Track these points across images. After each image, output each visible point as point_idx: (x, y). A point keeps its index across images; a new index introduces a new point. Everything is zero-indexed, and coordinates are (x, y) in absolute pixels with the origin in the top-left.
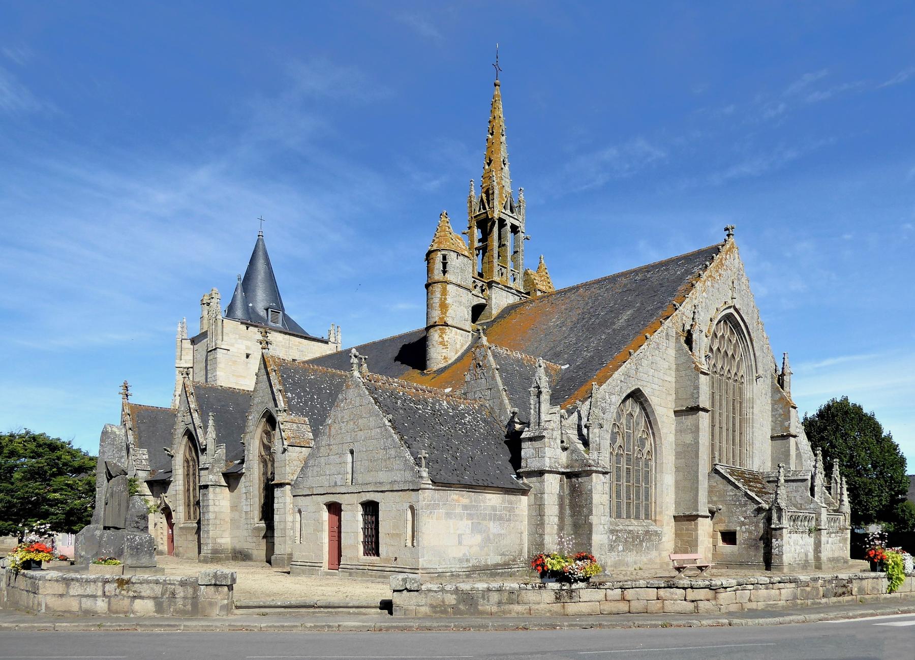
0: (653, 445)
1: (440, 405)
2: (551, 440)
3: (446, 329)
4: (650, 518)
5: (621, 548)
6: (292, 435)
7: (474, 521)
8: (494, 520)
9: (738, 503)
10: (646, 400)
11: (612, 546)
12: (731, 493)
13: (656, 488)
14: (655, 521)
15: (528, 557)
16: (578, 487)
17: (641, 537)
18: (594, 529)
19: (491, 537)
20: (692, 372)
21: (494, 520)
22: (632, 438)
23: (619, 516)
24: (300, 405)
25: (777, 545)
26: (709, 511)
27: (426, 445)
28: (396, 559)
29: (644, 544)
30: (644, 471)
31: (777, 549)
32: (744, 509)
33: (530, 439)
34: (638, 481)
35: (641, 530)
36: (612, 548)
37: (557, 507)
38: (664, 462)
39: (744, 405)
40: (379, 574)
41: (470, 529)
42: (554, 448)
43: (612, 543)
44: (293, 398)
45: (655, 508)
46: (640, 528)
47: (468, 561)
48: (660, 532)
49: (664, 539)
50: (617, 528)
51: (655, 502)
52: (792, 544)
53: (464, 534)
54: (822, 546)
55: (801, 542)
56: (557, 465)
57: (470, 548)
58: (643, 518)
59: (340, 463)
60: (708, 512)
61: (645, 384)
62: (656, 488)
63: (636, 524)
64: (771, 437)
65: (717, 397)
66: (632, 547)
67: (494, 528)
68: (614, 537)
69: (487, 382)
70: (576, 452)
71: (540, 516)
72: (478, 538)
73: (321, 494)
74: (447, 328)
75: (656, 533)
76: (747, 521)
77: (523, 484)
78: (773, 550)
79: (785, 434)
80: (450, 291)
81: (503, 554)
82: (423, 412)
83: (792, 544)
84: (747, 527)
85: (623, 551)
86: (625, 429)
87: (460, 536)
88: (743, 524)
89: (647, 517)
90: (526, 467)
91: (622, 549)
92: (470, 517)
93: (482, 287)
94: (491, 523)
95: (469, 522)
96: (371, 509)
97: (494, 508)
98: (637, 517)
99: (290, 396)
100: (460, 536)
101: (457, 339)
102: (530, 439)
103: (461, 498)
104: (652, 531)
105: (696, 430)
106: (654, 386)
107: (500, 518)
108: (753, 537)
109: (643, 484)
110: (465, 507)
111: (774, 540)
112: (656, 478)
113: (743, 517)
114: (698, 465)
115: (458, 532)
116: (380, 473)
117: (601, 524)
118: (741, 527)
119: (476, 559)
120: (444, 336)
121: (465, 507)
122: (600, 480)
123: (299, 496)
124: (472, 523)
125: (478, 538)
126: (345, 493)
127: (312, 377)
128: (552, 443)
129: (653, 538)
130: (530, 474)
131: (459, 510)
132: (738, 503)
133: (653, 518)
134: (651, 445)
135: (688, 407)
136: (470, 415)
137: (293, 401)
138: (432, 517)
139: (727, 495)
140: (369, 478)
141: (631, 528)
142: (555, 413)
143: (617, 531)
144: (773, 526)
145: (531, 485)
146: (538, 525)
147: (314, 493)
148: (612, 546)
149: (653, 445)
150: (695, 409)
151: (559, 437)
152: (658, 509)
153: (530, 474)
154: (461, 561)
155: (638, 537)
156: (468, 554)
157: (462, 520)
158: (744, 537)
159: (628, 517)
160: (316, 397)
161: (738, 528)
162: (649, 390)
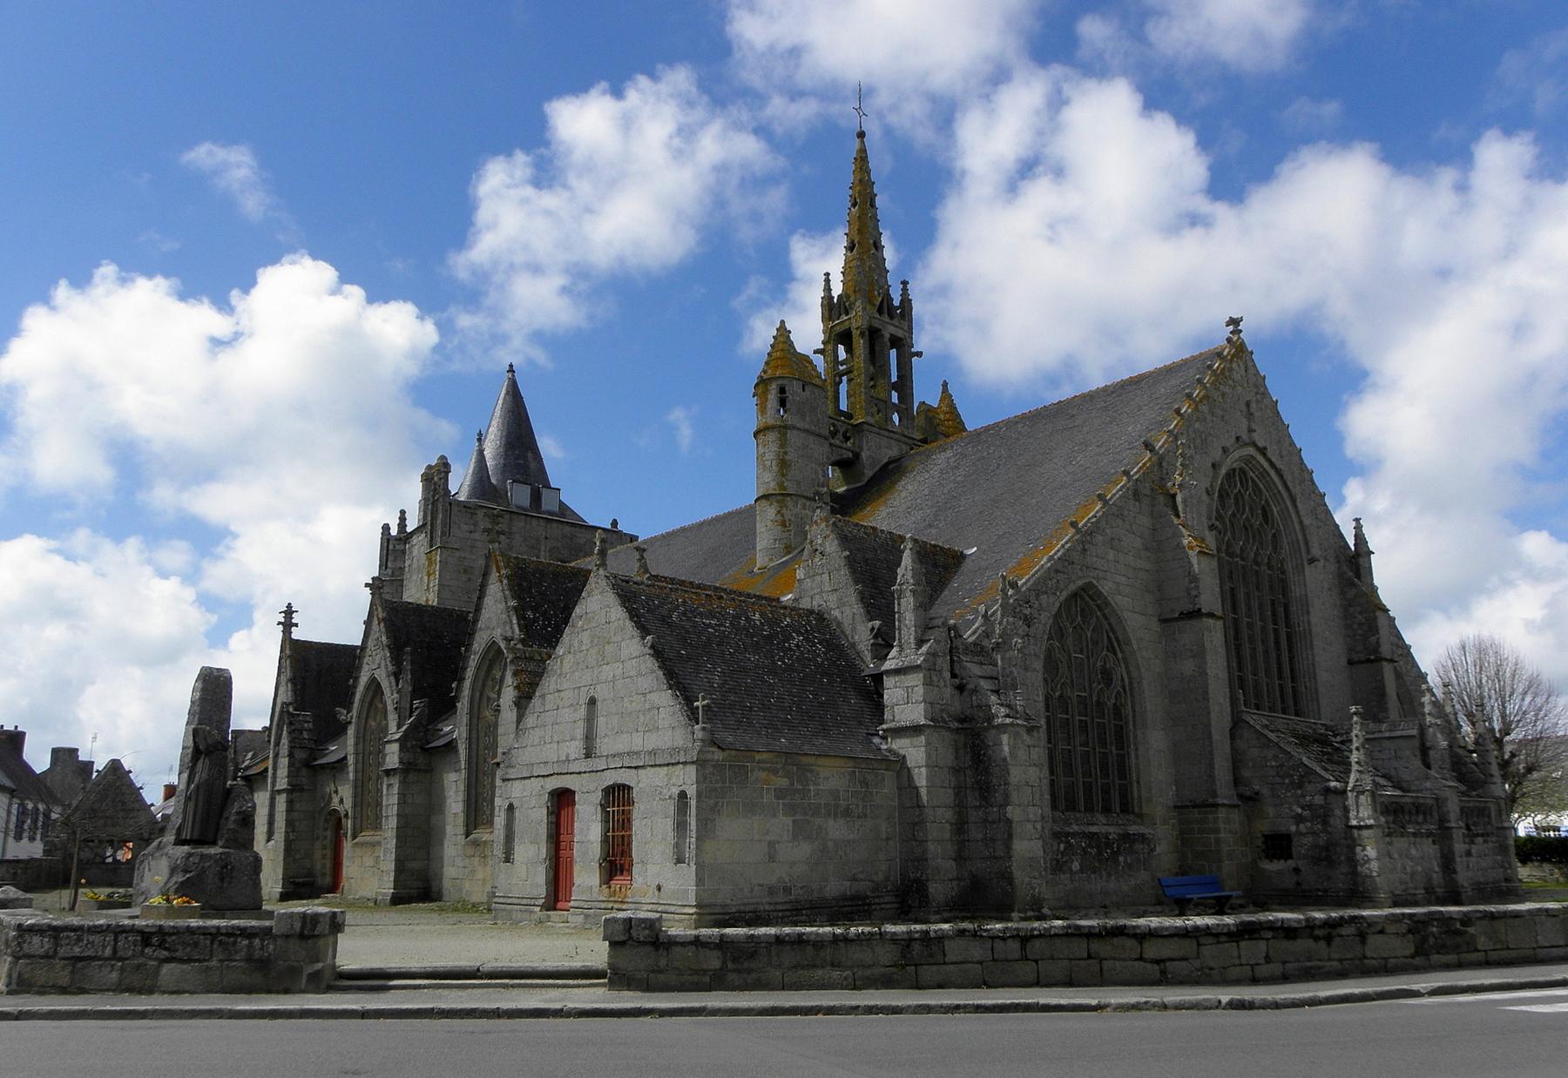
0: (1127, 681)
1: (747, 618)
2: (932, 672)
4: (1130, 809)
5: (1076, 866)
7: (797, 818)
8: (836, 815)
9: (1287, 781)
10: (1107, 604)
11: (1058, 861)
12: (1274, 763)
13: (1137, 756)
14: (1141, 816)
15: (902, 884)
17: (1115, 846)
18: (1017, 829)
19: (830, 844)
21: (836, 815)
22: (1086, 667)
23: (1072, 806)
26: (1237, 795)
27: (716, 685)
28: (659, 888)
29: (1121, 859)
30: (1112, 726)
33: (897, 672)
34: (1103, 743)
35: (1113, 831)
36: (1058, 866)
37: (950, 791)
38: (1148, 708)
39: (1293, 609)
41: (791, 832)
42: (937, 686)
43: (1060, 857)
44: (535, 620)
45: (1139, 791)
46: (1111, 829)
47: (787, 890)
48: (1150, 837)
49: (1158, 850)
50: (1067, 829)
51: (1138, 782)
52: (1396, 856)
53: (778, 843)
54: (1458, 859)
55: (1413, 852)
56: (945, 716)
57: (791, 867)
58: (1118, 810)
59: (575, 722)
60: (1235, 798)
61: (1101, 574)
62: (1137, 756)
63: (1104, 822)
64: (1349, 663)
65: (1241, 596)
66: (1097, 865)
67: (837, 830)
68: (1062, 846)
69: (830, 579)
72: (805, 849)
73: (543, 776)
74: (788, 498)
75: (1143, 838)
76: (1306, 813)
77: (889, 750)
78: (1359, 868)
79: (1372, 657)
81: (854, 879)
82: (716, 631)
83: (1396, 856)
85: (1082, 871)
86: (1072, 651)
87: (771, 844)
88: (1299, 819)
89: (1126, 808)
90: (893, 721)
91: (1078, 868)
92: (791, 809)
93: (846, 432)
94: (831, 822)
95: (788, 820)
96: (618, 798)
97: (835, 794)
98: (1107, 810)
100: (771, 844)
101: (807, 515)
102: (897, 672)
103: (772, 777)
104: (1134, 834)
105: (1199, 654)
106: (1118, 578)
107: (847, 813)
109: (1114, 748)
110: (780, 793)
112: (1136, 737)
113: (1299, 806)
114: (1209, 714)
115: (768, 838)
117: (1028, 821)
118: (1298, 825)
119: (802, 888)
120: (784, 511)
121: (780, 793)
122: (1023, 742)
124: (794, 821)
125: (805, 849)
128: (935, 678)
129: (1138, 846)
130: (900, 732)
131: (768, 798)
132: (1287, 781)
133: (1136, 809)
134: (1123, 680)
135: (1182, 613)
136: (799, 634)
138: (719, 811)
139: (1267, 766)
141: (1094, 829)
142: (939, 627)
143: (1068, 834)
144: (1354, 823)
145: (902, 752)
148: (1058, 861)
149: (1127, 681)
150: (1196, 614)
151: (946, 667)
152: (1144, 794)
153: (900, 732)
154: (771, 891)
155: (1108, 845)
156: (787, 879)
157: (774, 815)
159: (1090, 809)
162: (1110, 584)
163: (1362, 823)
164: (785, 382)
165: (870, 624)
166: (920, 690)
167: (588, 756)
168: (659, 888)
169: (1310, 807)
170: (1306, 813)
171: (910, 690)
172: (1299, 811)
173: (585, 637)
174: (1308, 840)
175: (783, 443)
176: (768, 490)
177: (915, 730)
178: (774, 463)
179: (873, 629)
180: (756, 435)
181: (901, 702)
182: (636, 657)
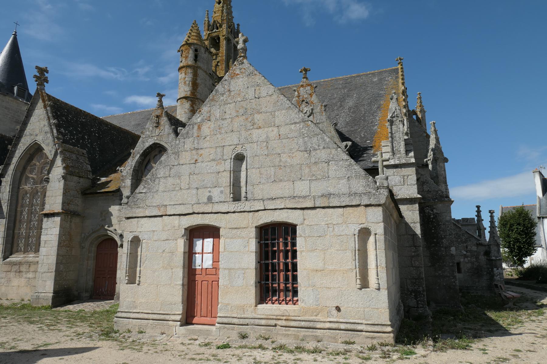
3: (196, 101)
6: (71, 164)
9: (459, 240)
16: (434, 218)
20: (424, 139)
24: (72, 142)
25: (498, 273)
28: (338, 309)
31: (499, 276)
32: (465, 245)
40: (303, 334)
70: (428, 183)
71: (415, 247)
76: (468, 254)
78: (495, 277)
80: (200, 75)
84: (469, 259)
88: (465, 256)
99: (64, 132)
108: (475, 267)
111: (495, 269)
116: (298, 184)
118: (464, 259)
120: (194, 106)
123: (138, 217)
126: (258, 211)
127: (84, 120)
137: (66, 137)
140: (276, 190)
146: (413, 257)
147: (168, 213)
158: (468, 267)
160: (86, 138)
161: (462, 260)
163: (497, 258)
164: (198, 47)
165: (345, 143)
166: (413, 178)
167: (237, 198)
168: (338, 309)
169: (471, 251)
170: (468, 254)
171: (406, 177)
172: (465, 253)
173: (230, 109)
174: (469, 265)
175: (195, 75)
176: (186, 95)
177: (410, 201)
178: (190, 83)
179: (346, 146)
180: (179, 70)
181: (399, 184)
182: (295, 123)
